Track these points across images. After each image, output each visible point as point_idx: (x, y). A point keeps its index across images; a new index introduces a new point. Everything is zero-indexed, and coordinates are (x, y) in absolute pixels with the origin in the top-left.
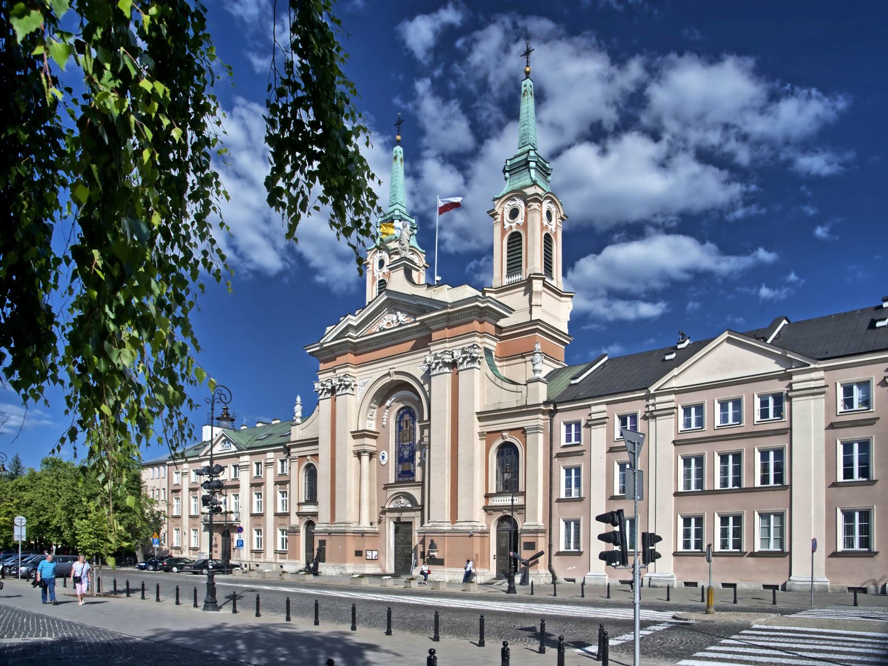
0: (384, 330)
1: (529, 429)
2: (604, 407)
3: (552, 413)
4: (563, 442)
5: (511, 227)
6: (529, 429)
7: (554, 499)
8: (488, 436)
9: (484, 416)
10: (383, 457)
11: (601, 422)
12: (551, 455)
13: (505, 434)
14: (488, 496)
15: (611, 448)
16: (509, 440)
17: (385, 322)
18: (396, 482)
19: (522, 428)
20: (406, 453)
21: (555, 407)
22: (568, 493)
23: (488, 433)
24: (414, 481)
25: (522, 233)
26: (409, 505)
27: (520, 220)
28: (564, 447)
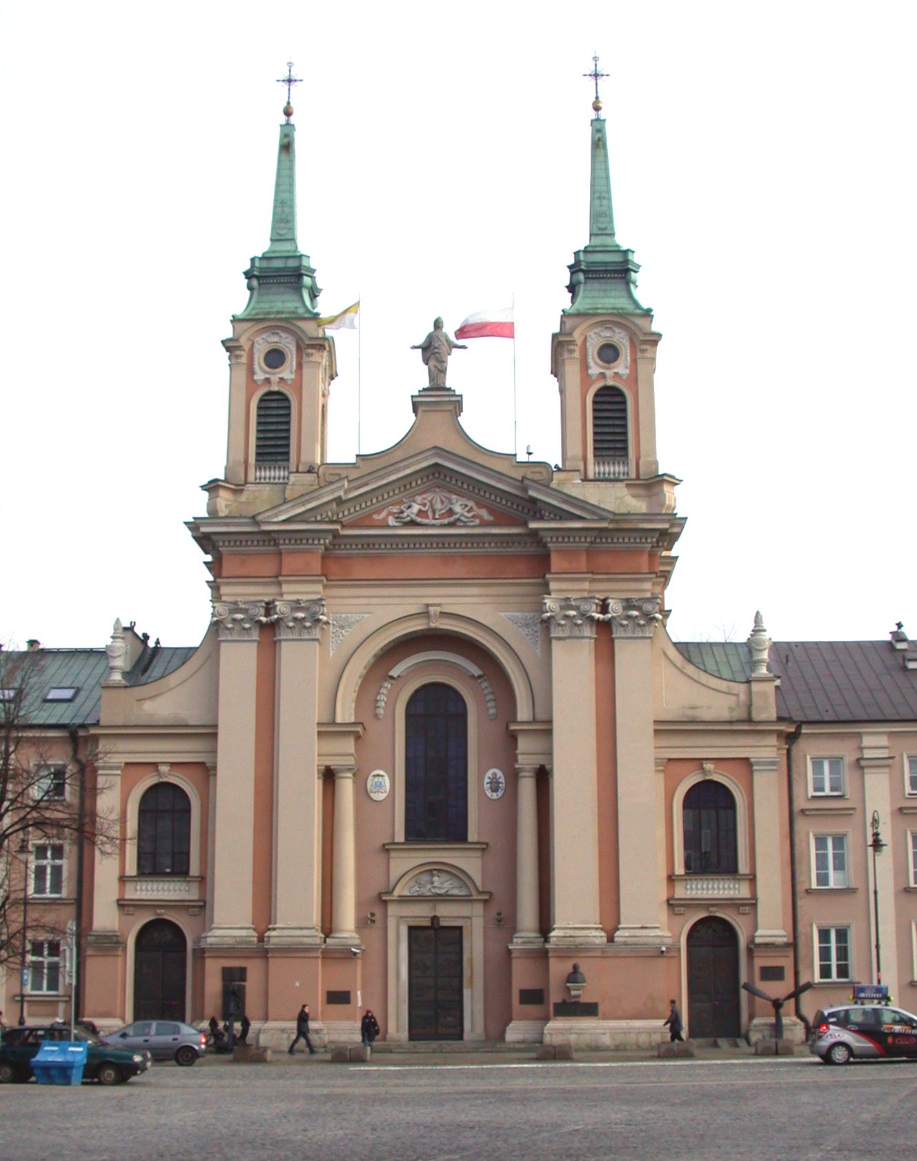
0: (413, 523)
1: (758, 763)
2: (883, 741)
3: (791, 738)
4: (811, 793)
5: (603, 376)
6: (758, 763)
7: (800, 888)
8: (669, 765)
9: (665, 729)
11: (884, 764)
13: (709, 766)
14: (671, 879)
15: (901, 809)
16: (716, 778)
17: (416, 508)
19: (747, 759)
22: (823, 879)
23: (670, 760)
26: (455, 892)
27: (622, 367)
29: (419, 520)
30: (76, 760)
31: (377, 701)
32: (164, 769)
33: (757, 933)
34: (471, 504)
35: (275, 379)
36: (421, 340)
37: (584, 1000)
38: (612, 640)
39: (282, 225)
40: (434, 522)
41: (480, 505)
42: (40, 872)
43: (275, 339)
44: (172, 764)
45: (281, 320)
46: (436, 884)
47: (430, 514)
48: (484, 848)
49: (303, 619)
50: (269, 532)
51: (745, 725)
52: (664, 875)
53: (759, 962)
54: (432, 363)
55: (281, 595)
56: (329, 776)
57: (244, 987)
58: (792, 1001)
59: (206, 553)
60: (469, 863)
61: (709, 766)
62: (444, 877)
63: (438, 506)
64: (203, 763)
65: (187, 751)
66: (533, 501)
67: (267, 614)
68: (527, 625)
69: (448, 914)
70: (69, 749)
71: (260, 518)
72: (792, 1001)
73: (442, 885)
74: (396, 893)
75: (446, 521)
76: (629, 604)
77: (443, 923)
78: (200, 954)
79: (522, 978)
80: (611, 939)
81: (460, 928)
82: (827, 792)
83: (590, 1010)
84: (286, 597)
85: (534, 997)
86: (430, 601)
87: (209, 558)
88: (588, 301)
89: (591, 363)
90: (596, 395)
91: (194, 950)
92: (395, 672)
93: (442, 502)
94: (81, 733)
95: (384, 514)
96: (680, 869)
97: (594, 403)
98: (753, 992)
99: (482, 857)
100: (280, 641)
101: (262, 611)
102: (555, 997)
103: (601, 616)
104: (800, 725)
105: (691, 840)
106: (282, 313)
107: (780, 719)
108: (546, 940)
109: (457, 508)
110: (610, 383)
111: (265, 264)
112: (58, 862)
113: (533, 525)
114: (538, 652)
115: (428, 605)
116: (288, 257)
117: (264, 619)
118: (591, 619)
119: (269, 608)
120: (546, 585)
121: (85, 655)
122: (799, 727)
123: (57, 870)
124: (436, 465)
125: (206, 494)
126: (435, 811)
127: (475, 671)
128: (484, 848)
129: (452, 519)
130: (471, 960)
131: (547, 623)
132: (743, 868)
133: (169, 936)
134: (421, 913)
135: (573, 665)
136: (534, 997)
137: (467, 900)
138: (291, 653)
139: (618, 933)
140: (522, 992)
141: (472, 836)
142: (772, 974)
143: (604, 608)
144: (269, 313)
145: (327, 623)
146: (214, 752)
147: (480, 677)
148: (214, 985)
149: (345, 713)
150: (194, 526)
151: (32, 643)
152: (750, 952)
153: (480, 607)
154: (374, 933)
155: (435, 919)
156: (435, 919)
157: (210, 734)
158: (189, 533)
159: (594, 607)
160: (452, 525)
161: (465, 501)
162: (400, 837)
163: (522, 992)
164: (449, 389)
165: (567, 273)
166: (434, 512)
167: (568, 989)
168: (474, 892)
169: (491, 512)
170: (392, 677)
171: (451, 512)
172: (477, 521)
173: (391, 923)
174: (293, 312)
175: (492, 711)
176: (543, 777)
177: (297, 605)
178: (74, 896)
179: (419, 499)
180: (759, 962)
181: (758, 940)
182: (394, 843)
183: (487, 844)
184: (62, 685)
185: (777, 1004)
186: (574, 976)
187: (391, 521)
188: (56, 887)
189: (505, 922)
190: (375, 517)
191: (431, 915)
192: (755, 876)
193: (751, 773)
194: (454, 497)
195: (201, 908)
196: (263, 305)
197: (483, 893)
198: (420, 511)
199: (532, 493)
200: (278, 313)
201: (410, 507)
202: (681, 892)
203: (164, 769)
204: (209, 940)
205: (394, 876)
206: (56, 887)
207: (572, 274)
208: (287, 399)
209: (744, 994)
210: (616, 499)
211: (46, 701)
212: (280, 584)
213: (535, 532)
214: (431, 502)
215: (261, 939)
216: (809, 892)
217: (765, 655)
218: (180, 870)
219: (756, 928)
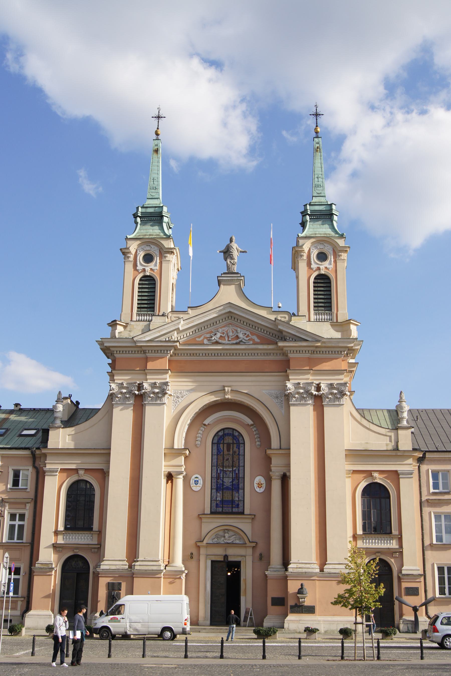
0: (217, 343)
1: (403, 474)
3: (421, 460)
4: (432, 490)
6: (403, 474)
10: (196, 482)
12: (421, 500)
13: (376, 475)
14: (355, 537)
17: (219, 335)
18: (212, 513)
19: (396, 471)
20: (228, 481)
21: (424, 454)
22: (439, 539)
23: (353, 471)
24: (243, 513)
25: (332, 276)
26: (238, 542)
28: (434, 494)
29: (220, 341)
30: (34, 466)
31: (196, 437)
32: (81, 472)
33: (403, 568)
34: (248, 333)
35: (148, 269)
36: (223, 248)
37: (306, 604)
38: (323, 406)
39: (153, 191)
40: (228, 342)
41: (252, 334)
42: (12, 527)
43: (148, 248)
44: (86, 470)
45: (151, 238)
46: (227, 537)
47: (226, 338)
48: (253, 517)
49: (158, 393)
50: (141, 347)
51: (396, 453)
52: (351, 534)
53: (404, 585)
54: (228, 261)
55: (147, 380)
56: (170, 477)
57: (120, 593)
58: (424, 607)
59: (108, 358)
60: (244, 525)
61: (376, 475)
62: (231, 533)
63: (231, 334)
64: (103, 469)
65: (94, 463)
66: (281, 331)
67: (139, 390)
68: (277, 397)
69: (234, 554)
70: (30, 462)
71: (135, 339)
72: (424, 607)
73: (229, 538)
74: (205, 542)
75: (235, 342)
76: (331, 386)
77: (230, 559)
78: (97, 576)
79: (273, 592)
80: (322, 570)
81: (239, 562)
82: (441, 489)
83: (311, 610)
84: (149, 381)
85: (280, 601)
86: (225, 384)
87: (110, 361)
88: (311, 230)
89: (313, 262)
90: (315, 279)
91: (94, 572)
92: (206, 422)
93: (233, 332)
94: (38, 452)
95: (202, 338)
96: (360, 531)
97: (314, 283)
98: (401, 603)
99: (252, 523)
100: (145, 404)
101: (136, 388)
102: (291, 602)
103: (317, 393)
104: (425, 453)
105: (366, 515)
106: (152, 235)
107: (414, 450)
108: (286, 570)
109: (241, 335)
110: (323, 272)
111: (144, 210)
112: (21, 523)
113: (281, 344)
114: (283, 411)
115: (224, 387)
116: (155, 207)
117: (137, 392)
118: (312, 394)
119: (140, 387)
120: (288, 376)
121: (43, 413)
122: (424, 454)
123: (21, 527)
124: (230, 312)
125: (110, 328)
126: (226, 497)
127: (250, 422)
128: (253, 517)
129: (238, 341)
130: (245, 580)
131: (288, 397)
132: (395, 532)
133: (80, 564)
134: (218, 553)
135: (302, 418)
136: (280, 601)
137: (243, 545)
138: (150, 411)
139: (326, 567)
140: (273, 599)
141: (247, 511)
142: (413, 592)
143: (318, 388)
144: (145, 235)
145: (170, 395)
146: (108, 462)
147: (252, 425)
148: (102, 593)
149: (179, 443)
150: (101, 343)
151: (17, 405)
152: (399, 578)
153: (252, 388)
154: (193, 563)
155: (226, 556)
156: (226, 556)
157: (106, 453)
158: (99, 347)
159: (313, 388)
160: (236, 344)
161: (245, 332)
162: (208, 511)
163: (273, 599)
164: (237, 273)
165: (300, 216)
166: (228, 337)
167: (298, 598)
168: (247, 542)
169: (258, 337)
170: (205, 425)
171: (237, 337)
172: (251, 342)
173: (202, 559)
174: (158, 235)
175: (258, 443)
176: (285, 479)
177: (154, 385)
178: (29, 541)
179: (220, 330)
180: (404, 585)
181: (404, 572)
182: (204, 514)
183: (255, 515)
184: (30, 427)
185: (415, 609)
186: (301, 591)
187: (206, 342)
188: (20, 537)
189: (264, 558)
190: (197, 339)
191: (224, 554)
192: (401, 536)
193: (399, 479)
194: (239, 330)
195: (99, 549)
196: (142, 231)
197: (252, 542)
198: (221, 336)
199: (280, 327)
200: (150, 235)
201: (215, 334)
202: (360, 544)
203: (81, 472)
204: (102, 567)
205: (204, 534)
206: (20, 537)
207: (303, 216)
208: (154, 280)
209: (396, 602)
210: (326, 331)
211: (21, 435)
212: (146, 374)
213: (281, 348)
214: (227, 331)
215: (130, 566)
216: (431, 545)
217: (405, 415)
218: (88, 528)
219: (402, 566)
